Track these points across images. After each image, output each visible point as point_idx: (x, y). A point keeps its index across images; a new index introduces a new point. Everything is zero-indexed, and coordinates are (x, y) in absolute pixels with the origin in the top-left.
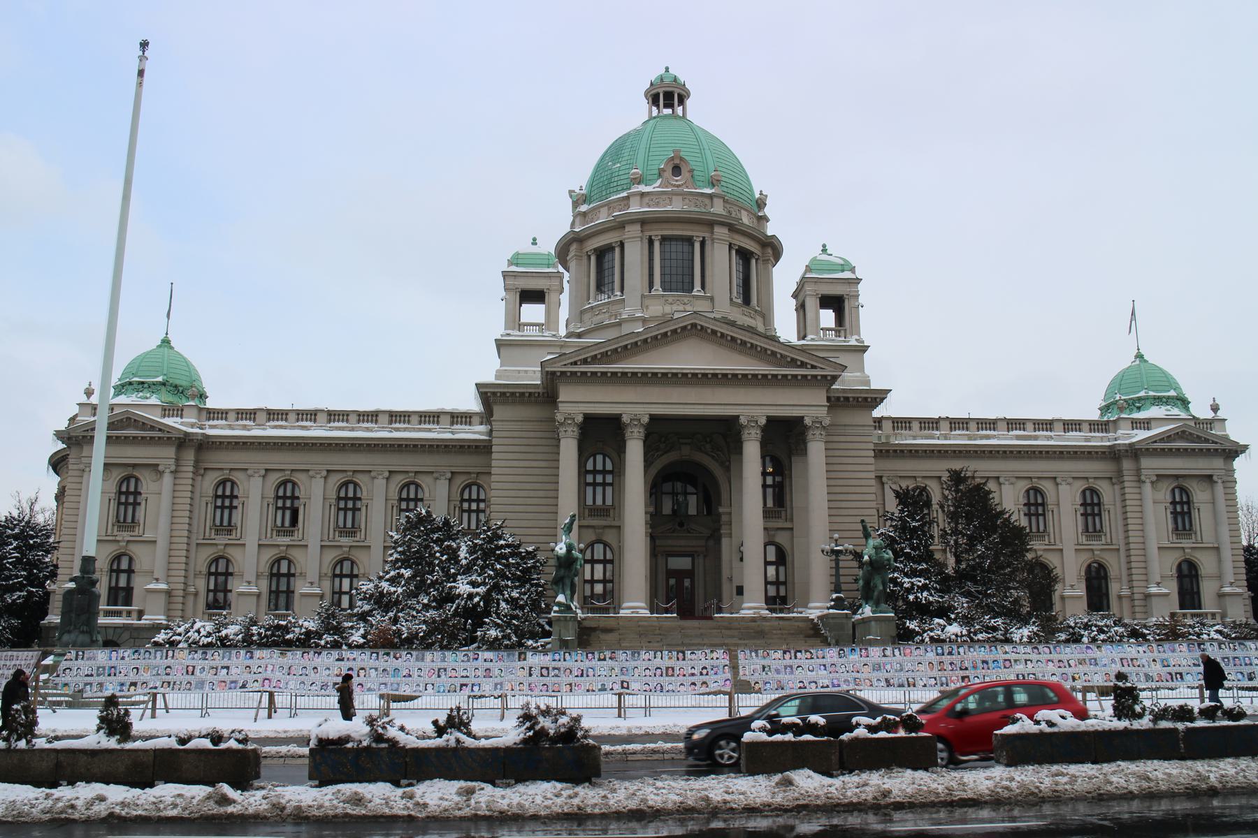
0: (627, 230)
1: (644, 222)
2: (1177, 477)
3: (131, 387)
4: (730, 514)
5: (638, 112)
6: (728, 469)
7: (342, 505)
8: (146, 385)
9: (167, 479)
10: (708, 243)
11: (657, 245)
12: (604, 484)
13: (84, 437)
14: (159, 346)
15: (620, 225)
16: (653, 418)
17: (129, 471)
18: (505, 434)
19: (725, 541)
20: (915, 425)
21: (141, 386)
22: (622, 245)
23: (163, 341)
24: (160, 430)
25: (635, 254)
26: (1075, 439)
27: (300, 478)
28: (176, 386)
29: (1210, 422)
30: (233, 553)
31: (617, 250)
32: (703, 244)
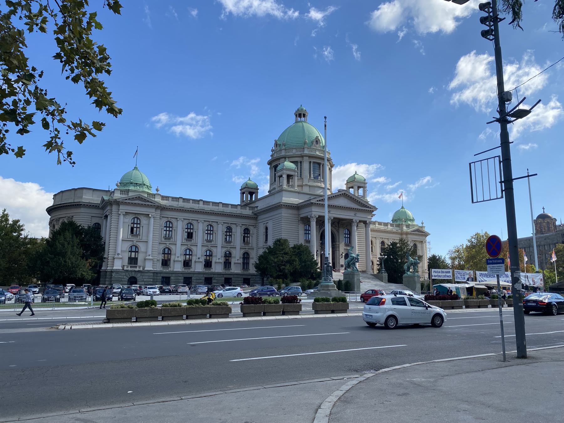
0: (304, 158)
1: (310, 157)
2: (415, 241)
4: (339, 245)
5: (292, 119)
6: (338, 232)
7: (171, 229)
9: (152, 220)
11: (312, 164)
12: (308, 234)
14: (133, 170)
15: (302, 157)
16: (334, 218)
17: (137, 216)
18: (285, 217)
19: (337, 251)
20: (383, 224)
22: (301, 163)
23: (135, 168)
24: (151, 202)
25: (306, 166)
26: (382, 227)
27: (194, 223)
28: (147, 186)
29: (422, 227)
30: (172, 247)
31: (299, 164)
32: (323, 165)
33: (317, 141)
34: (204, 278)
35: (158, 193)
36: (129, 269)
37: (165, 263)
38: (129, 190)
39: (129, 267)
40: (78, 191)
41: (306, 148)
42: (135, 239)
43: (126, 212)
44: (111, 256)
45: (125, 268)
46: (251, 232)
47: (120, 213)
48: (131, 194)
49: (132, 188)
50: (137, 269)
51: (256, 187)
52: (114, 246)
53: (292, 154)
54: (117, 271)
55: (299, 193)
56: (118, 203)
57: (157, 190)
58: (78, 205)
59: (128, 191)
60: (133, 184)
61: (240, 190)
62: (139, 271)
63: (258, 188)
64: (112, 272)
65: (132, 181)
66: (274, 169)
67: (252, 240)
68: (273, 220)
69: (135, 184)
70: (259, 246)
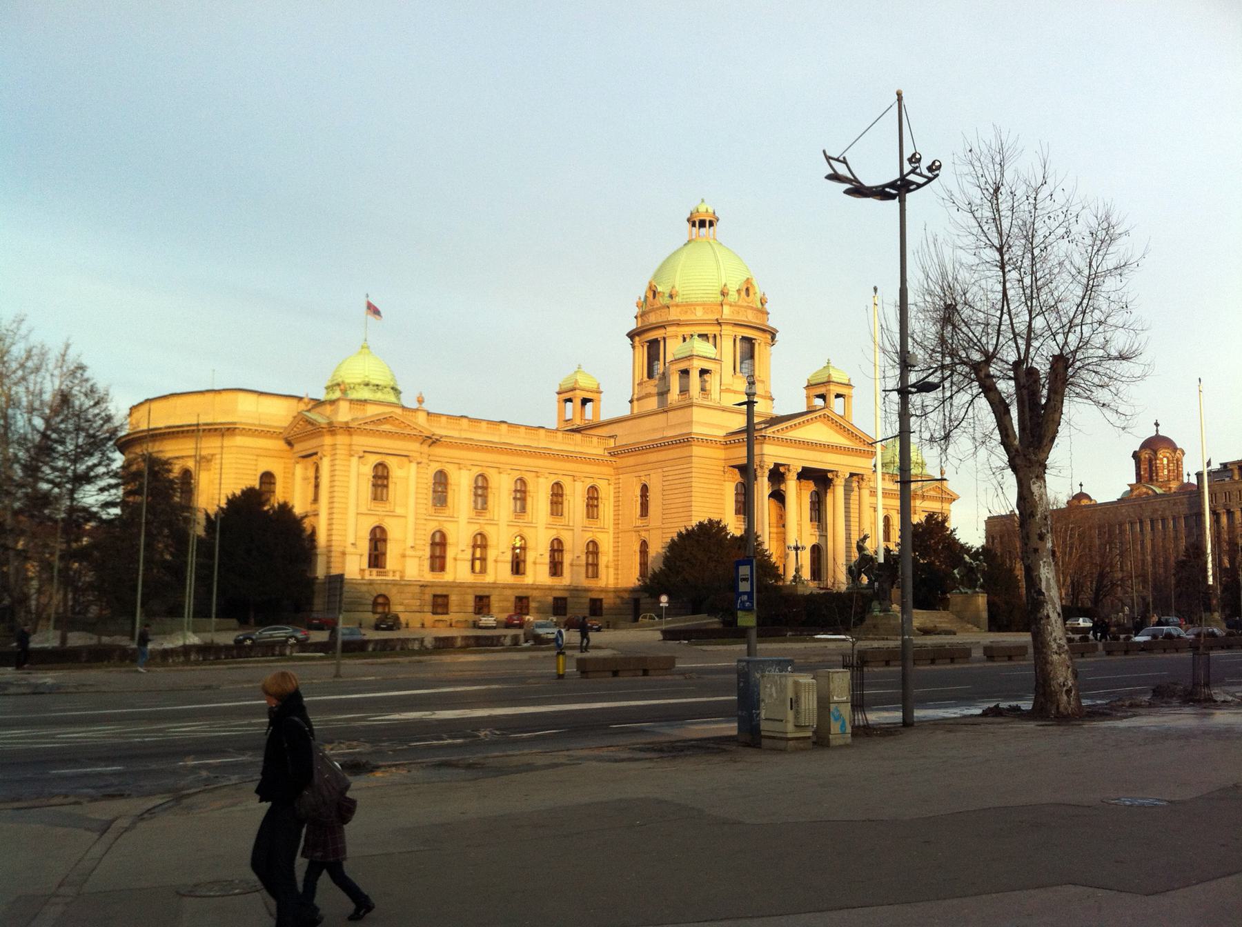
3: (366, 388)
8: (380, 388)
10: (762, 344)
16: (804, 468)
21: (375, 388)
23: (363, 347)
32: (759, 344)
33: (747, 289)
34: (513, 599)
35: (425, 406)
36: (374, 577)
37: (438, 562)
40: (225, 396)
41: (726, 304)
42: (380, 508)
45: (367, 577)
46: (602, 494)
47: (352, 453)
48: (371, 410)
49: (365, 394)
50: (390, 578)
51: (596, 387)
56: (348, 429)
57: (421, 401)
58: (226, 431)
60: (371, 387)
61: (559, 393)
62: (394, 583)
63: (601, 389)
66: (646, 348)
68: (665, 469)
69: (374, 385)
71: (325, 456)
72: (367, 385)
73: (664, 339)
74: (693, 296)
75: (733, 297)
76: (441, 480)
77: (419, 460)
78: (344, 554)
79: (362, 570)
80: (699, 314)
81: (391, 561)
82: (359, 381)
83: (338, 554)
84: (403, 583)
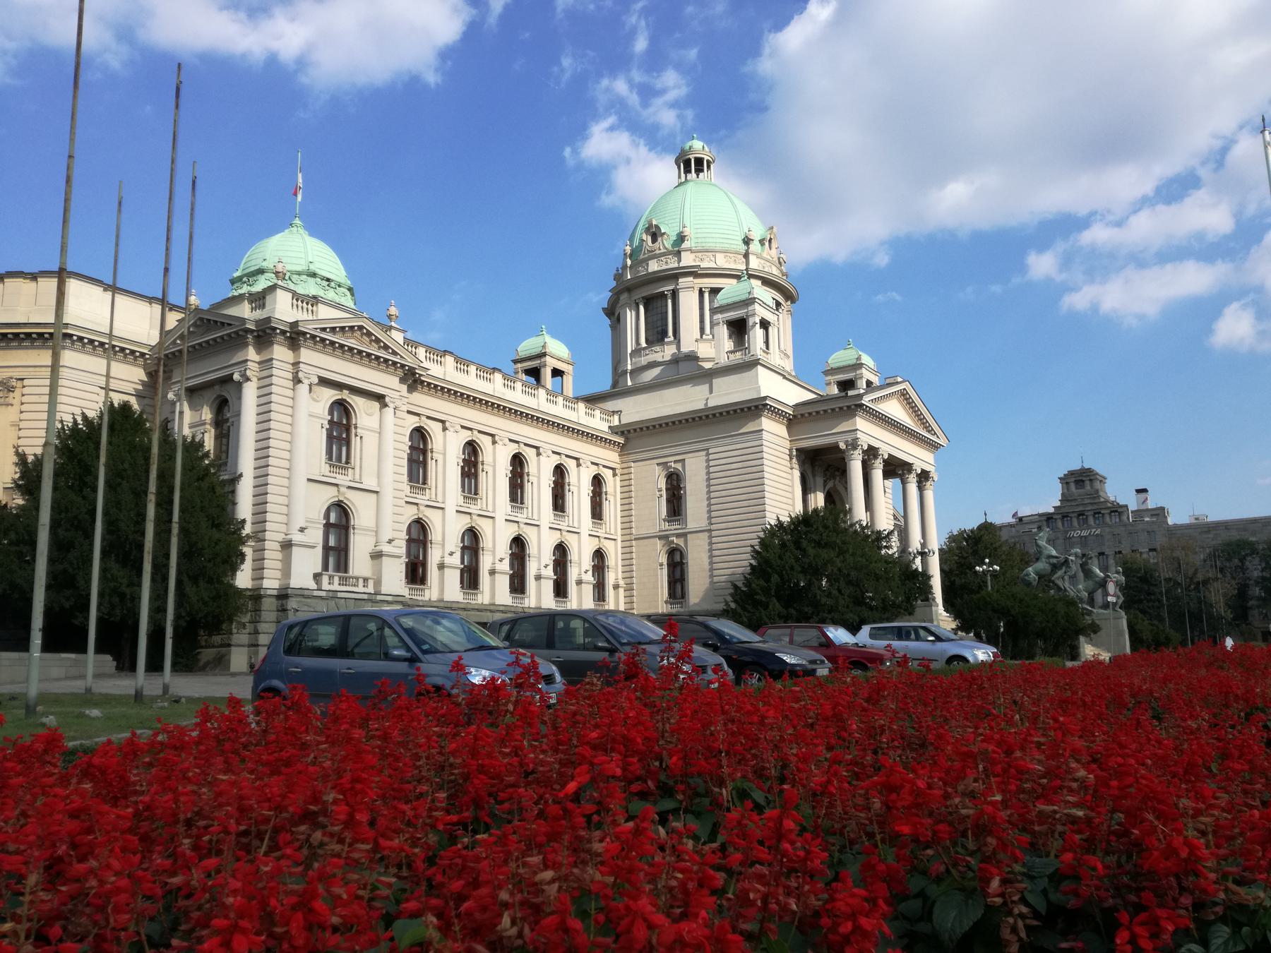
3: (311, 280)
8: (333, 284)
13: (313, 337)
17: (345, 395)
21: (325, 283)
24: (395, 353)
36: (336, 587)
37: (416, 573)
38: (314, 297)
39: (336, 580)
43: (319, 377)
44: (273, 536)
50: (360, 589)
52: (284, 500)
53: (712, 265)
54: (303, 594)
55: (784, 377)
56: (295, 337)
59: (315, 300)
64: (283, 595)
65: (313, 268)
67: (612, 508)
69: (323, 278)
70: (634, 531)
71: (248, 379)
72: (314, 275)
73: (675, 294)
74: (711, 240)
75: (755, 247)
76: (420, 441)
77: (398, 403)
78: (287, 546)
79: (317, 577)
80: (722, 262)
81: (359, 563)
82: (299, 268)
83: (277, 546)
84: (379, 598)
